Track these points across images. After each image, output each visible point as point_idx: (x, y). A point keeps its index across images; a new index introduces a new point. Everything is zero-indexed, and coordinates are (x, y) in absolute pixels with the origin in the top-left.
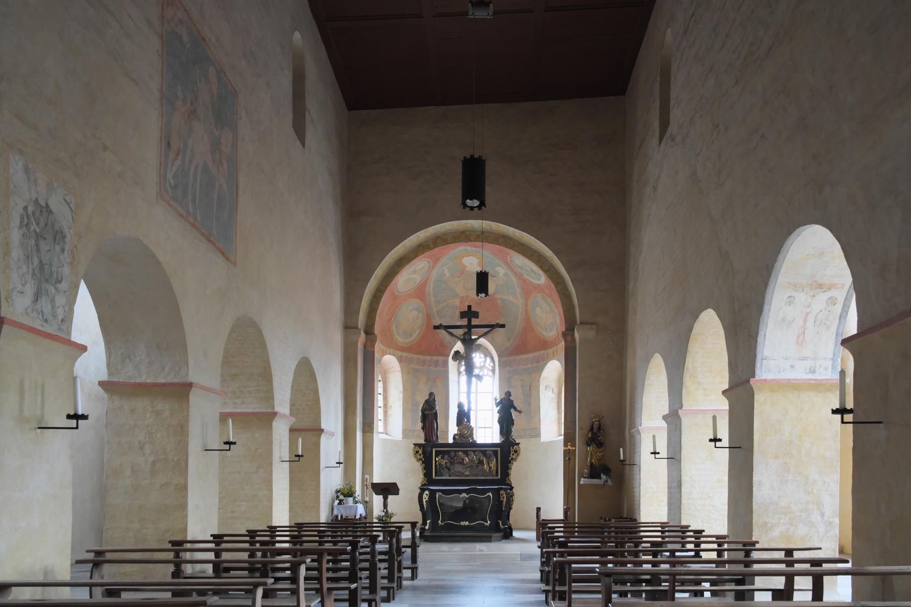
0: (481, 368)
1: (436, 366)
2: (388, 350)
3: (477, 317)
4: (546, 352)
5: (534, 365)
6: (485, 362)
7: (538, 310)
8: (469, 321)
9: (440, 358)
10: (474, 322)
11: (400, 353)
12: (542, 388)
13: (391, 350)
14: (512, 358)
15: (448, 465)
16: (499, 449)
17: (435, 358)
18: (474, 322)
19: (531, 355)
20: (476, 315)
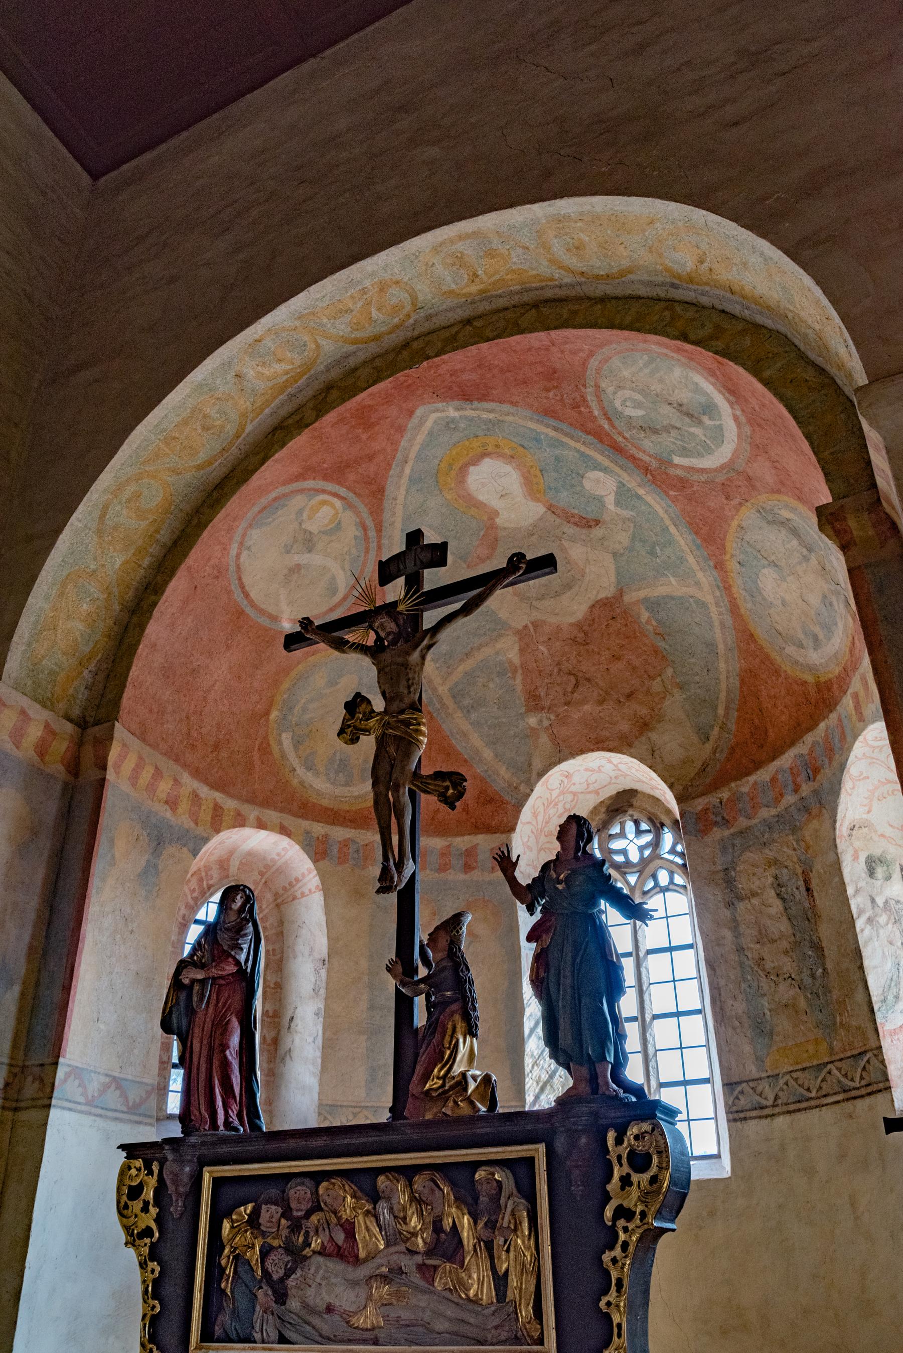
0: (645, 867)
1: (468, 868)
2: (252, 812)
3: (442, 562)
4: (833, 716)
5: (806, 789)
6: (656, 844)
7: (768, 580)
8: (414, 581)
9: (485, 843)
10: (433, 578)
11: (318, 829)
12: (852, 871)
13: (272, 815)
14: (725, 794)
15: (277, 1265)
16: (539, 1151)
17: (462, 842)
18: (433, 578)
19: (786, 760)
20: (438, 555)
